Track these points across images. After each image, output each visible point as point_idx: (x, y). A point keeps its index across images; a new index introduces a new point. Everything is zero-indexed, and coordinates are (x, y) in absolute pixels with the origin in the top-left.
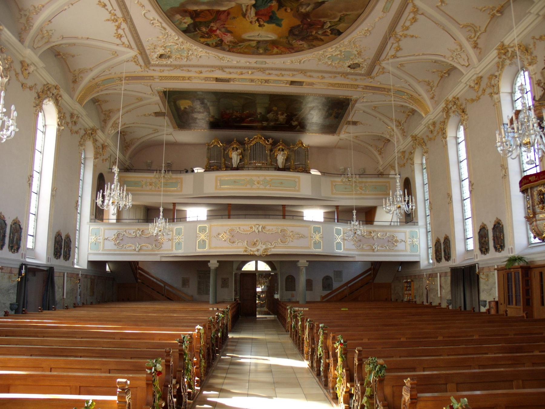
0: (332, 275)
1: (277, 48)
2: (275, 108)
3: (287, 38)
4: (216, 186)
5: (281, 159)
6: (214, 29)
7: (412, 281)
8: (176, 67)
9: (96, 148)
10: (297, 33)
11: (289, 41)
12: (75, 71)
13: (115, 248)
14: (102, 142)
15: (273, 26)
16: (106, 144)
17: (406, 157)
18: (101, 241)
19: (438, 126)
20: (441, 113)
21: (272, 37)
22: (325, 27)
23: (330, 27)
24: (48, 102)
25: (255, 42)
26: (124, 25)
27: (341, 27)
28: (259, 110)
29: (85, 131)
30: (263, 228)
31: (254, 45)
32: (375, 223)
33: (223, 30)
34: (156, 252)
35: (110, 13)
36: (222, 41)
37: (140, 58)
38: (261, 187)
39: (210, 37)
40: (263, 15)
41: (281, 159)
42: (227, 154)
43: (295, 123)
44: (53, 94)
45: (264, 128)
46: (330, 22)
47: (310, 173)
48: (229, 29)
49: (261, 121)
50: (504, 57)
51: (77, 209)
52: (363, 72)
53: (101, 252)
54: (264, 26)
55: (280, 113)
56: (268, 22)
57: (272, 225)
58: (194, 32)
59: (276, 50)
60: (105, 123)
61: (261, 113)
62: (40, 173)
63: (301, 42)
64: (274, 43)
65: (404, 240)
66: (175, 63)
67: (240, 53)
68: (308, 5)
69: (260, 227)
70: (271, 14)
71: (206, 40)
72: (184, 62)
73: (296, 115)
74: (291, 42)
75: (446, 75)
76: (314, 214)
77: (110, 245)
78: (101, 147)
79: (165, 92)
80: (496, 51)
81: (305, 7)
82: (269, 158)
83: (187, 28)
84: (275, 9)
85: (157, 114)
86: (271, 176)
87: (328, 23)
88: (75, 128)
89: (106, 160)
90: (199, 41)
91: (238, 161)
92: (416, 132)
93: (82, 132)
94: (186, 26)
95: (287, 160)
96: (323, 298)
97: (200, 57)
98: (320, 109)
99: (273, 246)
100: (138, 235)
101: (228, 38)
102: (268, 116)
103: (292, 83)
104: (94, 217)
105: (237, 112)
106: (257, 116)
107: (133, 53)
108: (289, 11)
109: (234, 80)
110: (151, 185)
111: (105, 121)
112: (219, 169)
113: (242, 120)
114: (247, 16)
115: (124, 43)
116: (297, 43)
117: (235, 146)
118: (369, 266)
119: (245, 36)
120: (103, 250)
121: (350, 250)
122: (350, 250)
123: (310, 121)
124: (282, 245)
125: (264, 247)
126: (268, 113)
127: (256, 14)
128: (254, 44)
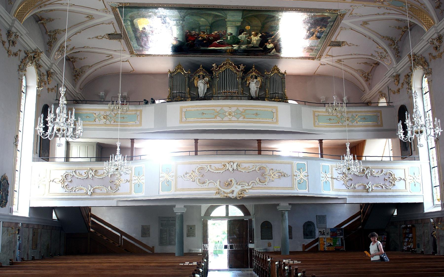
0: (314, 221)
4: (181, 118)
5: (254, 86)
7: (413, 226)
9: (40, 75)
14: (47, 68)
16: (52, 71)
17: (401, 81)
28: (229, 31)
32: (364, 159)
34: (112, 196)
38: (234, 119)
41: (254, 86)
43: (270, 46)
47: (288, 102)
49: (231, 44)
55: (253, 33)
57: (248, 162)
60: (51, 46)
65: (403, 178)
78: (45, 73)
82: (240, 86)
86: (246, 106)
89: (52, 89)
91: (205, 91)
95: (262, 88)
96: (305, 247)
99: (250, 187)
100: (90, 176)
102: (239, 37)
105: (204, 32)
106: (227, 38)
112: (183, 98)
113: (209, 42)
117: (201, 73)
118: (357, 210)
121: (339, 190)
122: (339, 190)
124: (261, 185)
125: (240, 188)
126: (240, 34)
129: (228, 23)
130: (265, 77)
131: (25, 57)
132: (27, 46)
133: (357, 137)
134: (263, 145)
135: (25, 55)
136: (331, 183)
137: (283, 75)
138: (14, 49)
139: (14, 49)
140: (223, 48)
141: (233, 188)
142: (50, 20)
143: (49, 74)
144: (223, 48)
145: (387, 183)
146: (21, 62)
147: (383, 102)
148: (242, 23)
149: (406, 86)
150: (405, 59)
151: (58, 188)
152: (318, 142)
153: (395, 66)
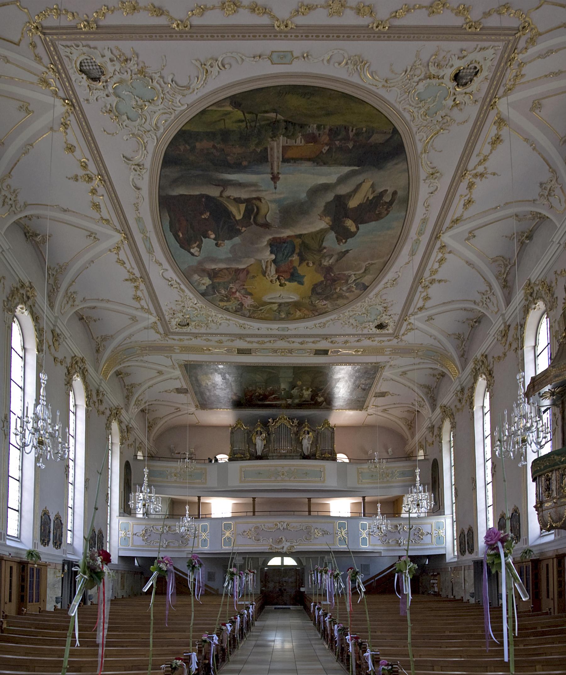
1: (300, 311)
2: (299, 383)
3: (310, 298)
8: (196, 336)
10: (320, 291)
11: (312, 302)
12: (98, 338)
13: (144, 543)
15: (295, 284)
19: (466, 391)
20: (470, 376)
22: (349, 282)
23: (355, 280)
24: (77, 378)
25: (276, 305)
26: (142, 286)
29: (110, 411)
30: (288, 525)
31: (276, 308)
35: (129, 272)
37: (159, 323)
40: (284, 272)
42: (251, 439)
44: (80, 368)
46: (355, 274)
48: (249, 290)
51: (108, 503)
52: (391, 331)
54: (286, 285)
56: (290, 280)
58: (212, 295)
61: (285, 389)
68: (331, 256)
69: (285, 524)
70: (292, 270)
72: (203, 330)
73: (322, 389)
74: (314, 303)
75: (477, 324)
76: (340, 507)
79: (186, 366)
81: (327, 259)
83: (205, 290)
84: (296, 264)
85: (179, 391)
87: (353, 276)
88: (102, 408)
89: (131, 445)
93: (108, 412)
94: (204, 287)
98: (346, 381)
100: (165, 531)
101: (248, 301)
104: (122, 511)
107: (153, 319)
108: (311, 265)
110: (175, 476)
111: (128, 398)
114: (267, 274)
115: (142, 308)
123: (337, 396)
127: (277, 271)
129: (281, 380)
130: (317, 432)
131: (110, 415)
133: (395, 493)
134: (313, 501)
135: (110, 413)
136: (371, 538)
140: (278, 402)
141: (283, 544)
144: (278, 402)
145: (416, 538)
148: (294, 379)
151: (139, 541)
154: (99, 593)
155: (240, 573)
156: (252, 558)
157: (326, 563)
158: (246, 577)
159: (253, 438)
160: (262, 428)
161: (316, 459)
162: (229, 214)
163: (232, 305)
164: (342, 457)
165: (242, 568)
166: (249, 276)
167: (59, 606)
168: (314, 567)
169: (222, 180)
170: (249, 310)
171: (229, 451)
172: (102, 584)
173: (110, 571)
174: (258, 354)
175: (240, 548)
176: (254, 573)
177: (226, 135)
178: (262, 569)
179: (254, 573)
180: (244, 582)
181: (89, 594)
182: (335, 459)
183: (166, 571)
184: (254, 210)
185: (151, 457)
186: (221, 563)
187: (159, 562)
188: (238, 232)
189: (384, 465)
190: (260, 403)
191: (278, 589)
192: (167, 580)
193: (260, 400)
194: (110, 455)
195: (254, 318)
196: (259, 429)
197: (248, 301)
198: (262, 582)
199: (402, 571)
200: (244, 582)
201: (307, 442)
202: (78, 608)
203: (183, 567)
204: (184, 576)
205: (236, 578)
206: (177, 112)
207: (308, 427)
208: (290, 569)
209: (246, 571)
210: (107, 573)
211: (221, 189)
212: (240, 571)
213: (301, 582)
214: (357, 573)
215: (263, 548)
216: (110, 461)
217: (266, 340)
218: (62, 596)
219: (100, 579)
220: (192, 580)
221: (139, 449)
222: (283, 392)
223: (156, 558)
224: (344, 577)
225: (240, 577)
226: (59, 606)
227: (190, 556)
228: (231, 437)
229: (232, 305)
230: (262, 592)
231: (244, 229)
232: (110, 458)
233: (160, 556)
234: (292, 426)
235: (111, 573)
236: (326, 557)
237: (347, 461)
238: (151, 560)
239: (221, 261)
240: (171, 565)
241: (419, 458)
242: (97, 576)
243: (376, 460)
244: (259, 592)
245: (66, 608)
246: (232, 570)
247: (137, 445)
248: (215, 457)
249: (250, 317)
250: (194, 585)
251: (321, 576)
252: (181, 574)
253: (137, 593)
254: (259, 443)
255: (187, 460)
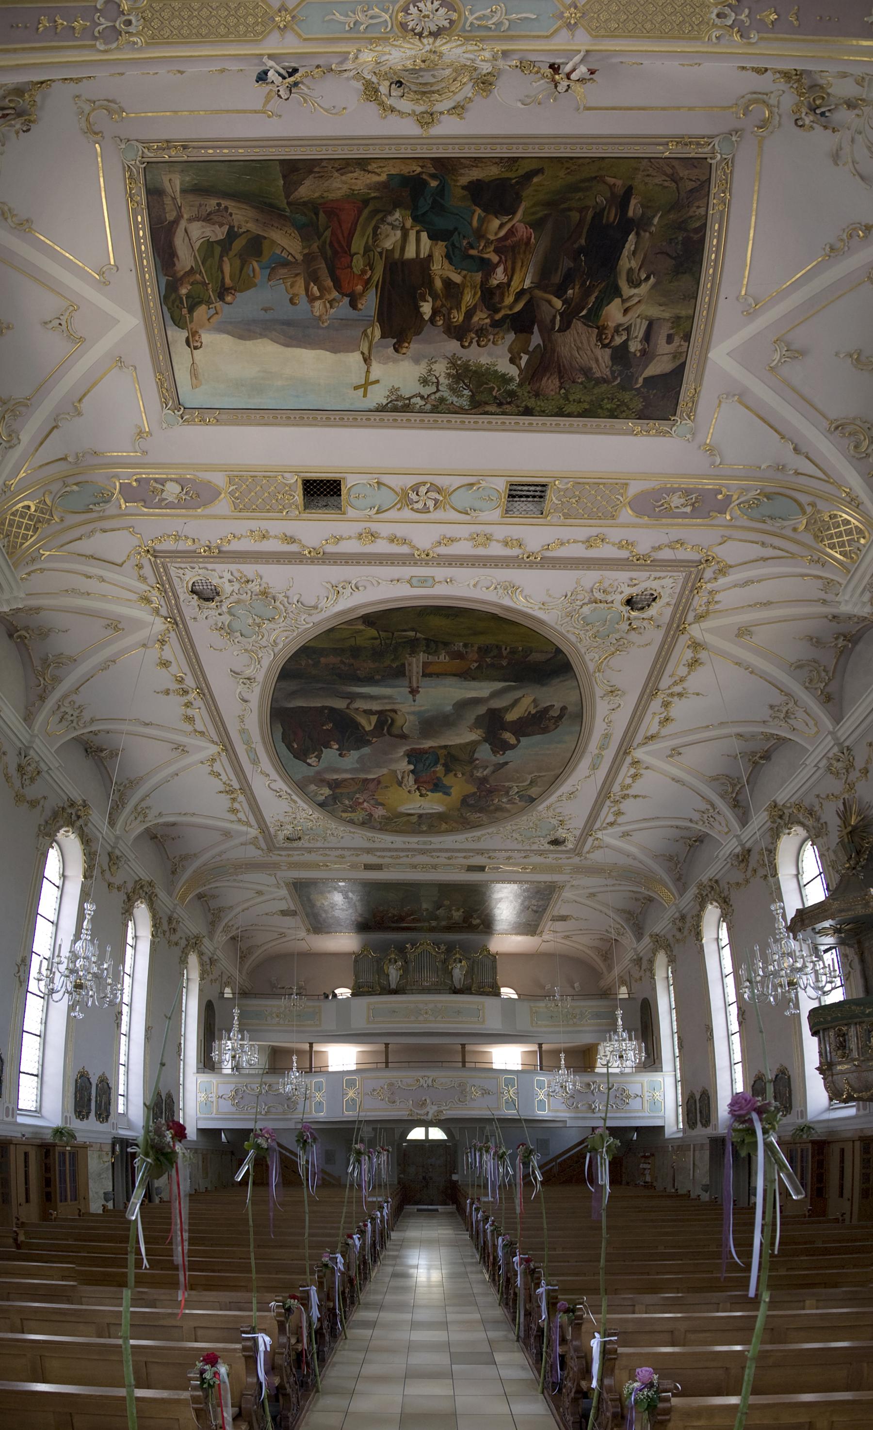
6: (361, 801)
9: (202, 964)
18: (214, 1099)
21: (439, 808)
27: (534, 791)
28: (424, 906)
33: (372, 802)
34: (289, 1116)
36: (371, 815)
39: (354, 811)
43: (476, 922)
45: (432, 930)
50: (779, 821)
53: (213, 1116)
59: (444, 826)
62: (130, 1005)
63: (479, 815)
64: (441, 817)
66: (307, 845)
67: (396, 831)
71: (349, 814)
77: (226, 1106)
78: (208, 962)
80: (766, 813)
90: (341, 818)
92: (657, 929)
97: (342, 838)
103: (471, 869)
109: (388, 866)
113: (401, 919)
116: (473, 817)
119: (403, 809)
120: (218, 1113)
128: (414, 819)
132: (187, 931)
137: (493, 958)
138: (174, 938)
139: (174, 938)
141: (428, 1109)
142: (214, 897)
143: (212, 962)
146: (183, 952)
147: (623, 992)
149: (648, 973)
150: (647, 940)
152: (537, 1046)
153: (635, 946)
154: (170, 1183)
155: (369, 1152)
156: (385, 1129)
157: (487, 1136)
158: (378, 1157)
159: (385, 967)
160: (396, 955)
161: (471, 994)
162: (357, 726)
163: (359, 816)
164: (507, 992)
165: (371, 1143)
166: (380, 786)
167: (110, 1205)
168: (470, 1143)
169: (350, 693)
170: (380, 823)
171: (351, 986)
172: (174, 1170)
173: (185, 1151)
174: (392, 869)
175: (368, 1114)
176: (388, 1151)
177: (356, 652)
178: (399, 1145)
179: (388, 1151)
180: (375, 1165)
181: (156, 1185)
182: (498, 994)
183: (267, 1149)
184: (387, 721)
185: (244, 994)
186: (341, 1136)
187: (257, 1136)
188: (368, 743)
189: (569, 1003)
190: (394, 925)
191: (421, 1177)
192: (269, 1163)
193: (393, 922)
194: (184, 994)
195: (386, 830)
196: (393, 956)
197: (379, 812)
198: (399, 1165)
199: (596, 1150)
200: (375, 1165)
201: (458, 972)
202: (140, 1208)
203: (290, 1142)
204: (293, 1157)
205: (365, 1159)
206: (300, 630)
207: (461, 955)
208: (438, 1146)
209: (378, 1148)
210: (180, 1155)
211: (349, 701)
212: (369, 1148)
213: (452, 1166)
214: (531, 1151)
215: (400, 1113)
216: (184, 1001)
217: (402, 854)
218: (113, 1190)
219: (172, 1164)
220: (303, 1162)
221: (227, 984)
222: (425, 913)
223: (252, 1130)
224: (513, 1158)
225: (369, 1157)
226: (110, 1205)
227: (299, 1126)
228: (355, 967)
229: (359, 816)
230: (399, 1179)
231: (375, 740)
232: (184, 998)
233: (258, 1127)
234: (437, 952)
235: (187, 1153)
236: (488, 1128)
237: (516, 997)
238: (245, 1134)
239: (346, 771)
240: (273, 1140)
241: (621, 996)
242: (167, 1160)
243: (557, 997)
244: (396, 1182)
245: (122, 1207)
246: (358, 1146)
247: (224, 980)
248: (333, 992)
249: (381, 829)
250: (307, 1169)
251: (481, 1156)
252: (288, 1154)
253: (226, 1184)
254: (394, 973)
255: (294, 996)
